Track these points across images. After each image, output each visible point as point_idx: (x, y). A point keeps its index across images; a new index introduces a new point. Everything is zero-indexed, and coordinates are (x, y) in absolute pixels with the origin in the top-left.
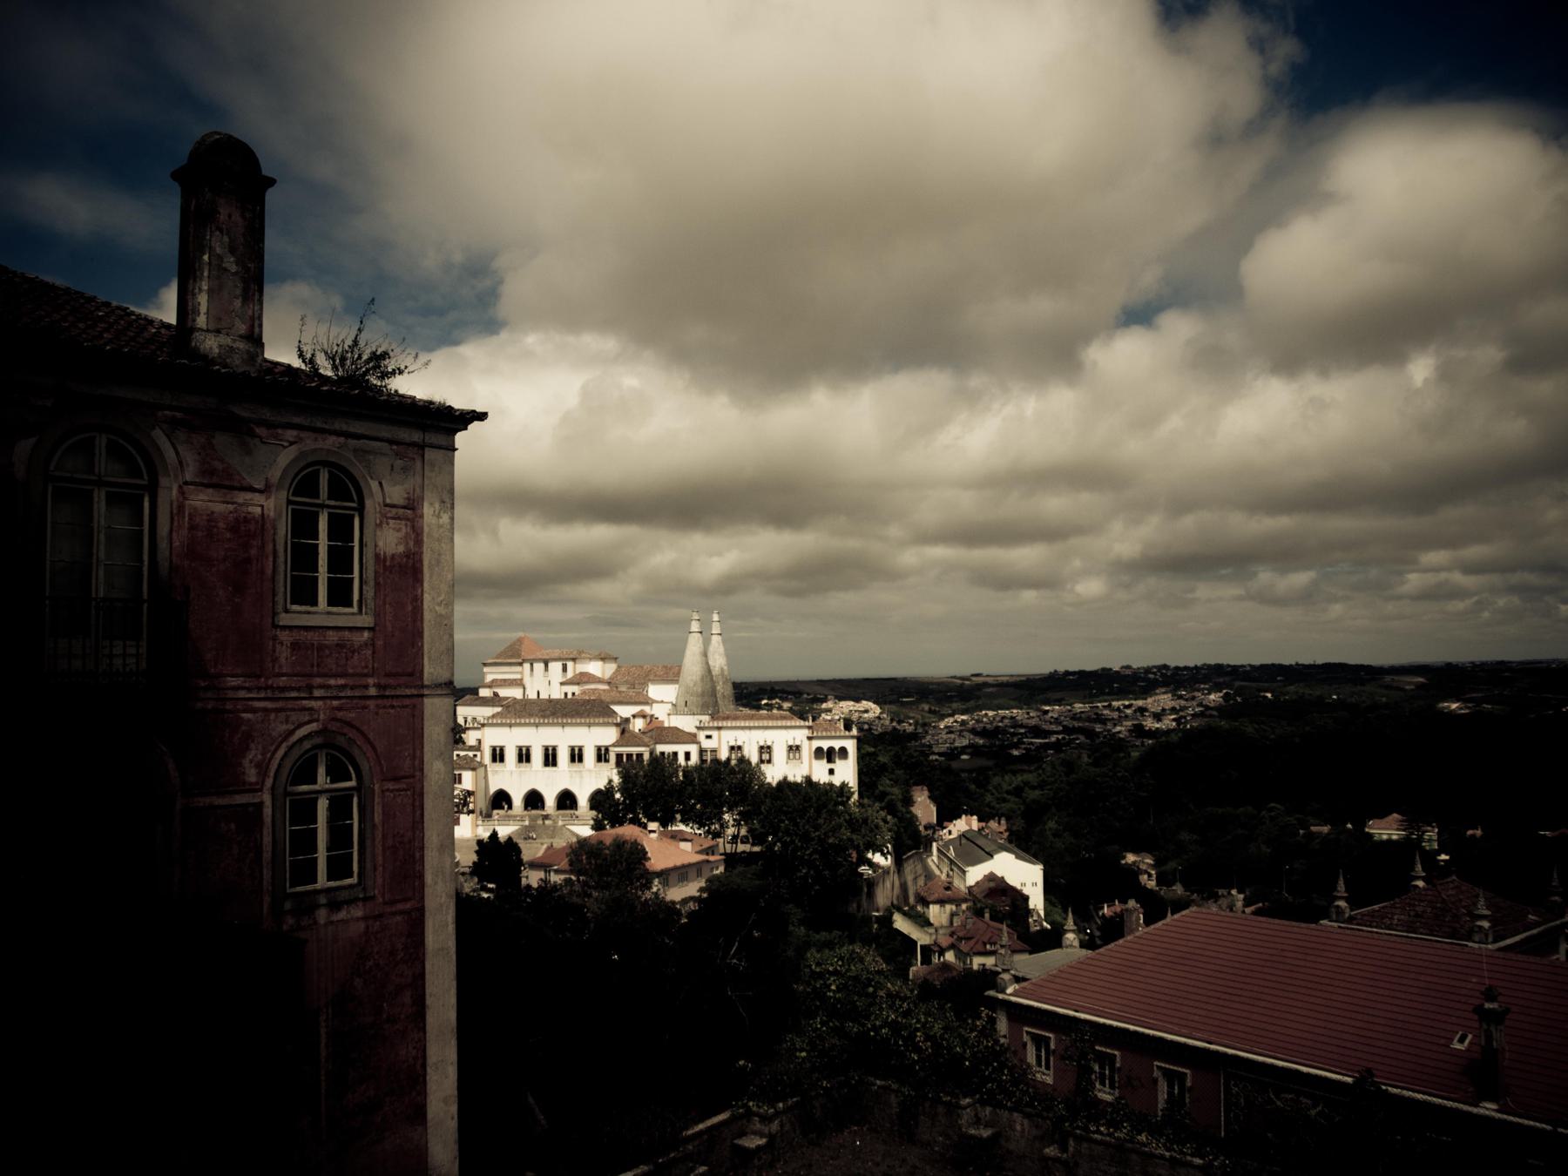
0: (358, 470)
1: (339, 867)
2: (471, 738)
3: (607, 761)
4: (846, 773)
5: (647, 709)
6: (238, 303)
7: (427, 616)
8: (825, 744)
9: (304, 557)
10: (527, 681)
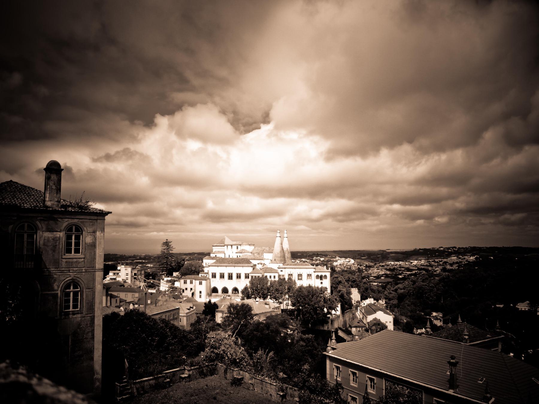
0: (81, 225)
1: (75, 306)
2: (206, 270)
3: (248, 278)
4: (327, 283)
5: (262, 262)
6: (55, 195)
7: (97, 255)
8: (320, 274)
9: (69, 244)
10: (225, 252)
